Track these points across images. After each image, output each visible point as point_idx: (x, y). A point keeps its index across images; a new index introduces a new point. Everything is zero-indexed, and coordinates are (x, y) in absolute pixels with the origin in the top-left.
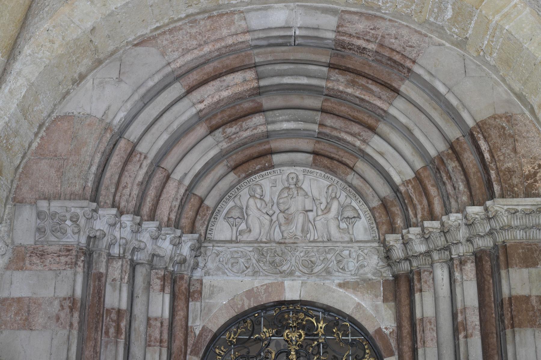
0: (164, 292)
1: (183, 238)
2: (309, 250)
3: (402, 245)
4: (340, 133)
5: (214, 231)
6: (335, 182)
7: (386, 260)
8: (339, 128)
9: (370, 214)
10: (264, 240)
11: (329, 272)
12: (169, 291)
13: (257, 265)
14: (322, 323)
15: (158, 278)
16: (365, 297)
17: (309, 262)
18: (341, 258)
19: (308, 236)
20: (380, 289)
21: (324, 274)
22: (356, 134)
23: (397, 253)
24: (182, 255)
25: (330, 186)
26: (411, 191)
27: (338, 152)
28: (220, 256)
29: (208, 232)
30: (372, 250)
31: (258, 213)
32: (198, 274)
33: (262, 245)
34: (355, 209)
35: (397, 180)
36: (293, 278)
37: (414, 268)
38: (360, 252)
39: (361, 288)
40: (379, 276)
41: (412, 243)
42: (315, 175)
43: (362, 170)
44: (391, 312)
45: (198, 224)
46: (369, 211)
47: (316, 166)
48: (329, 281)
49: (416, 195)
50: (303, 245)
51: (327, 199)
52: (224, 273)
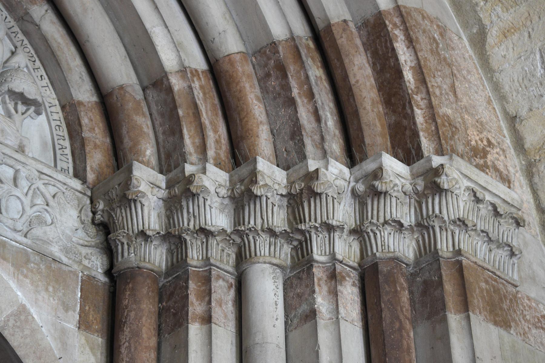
20: (75, 294)
23: (146, 218)
39: (32, 271)
41: (205, 200)
49: (206, 107)
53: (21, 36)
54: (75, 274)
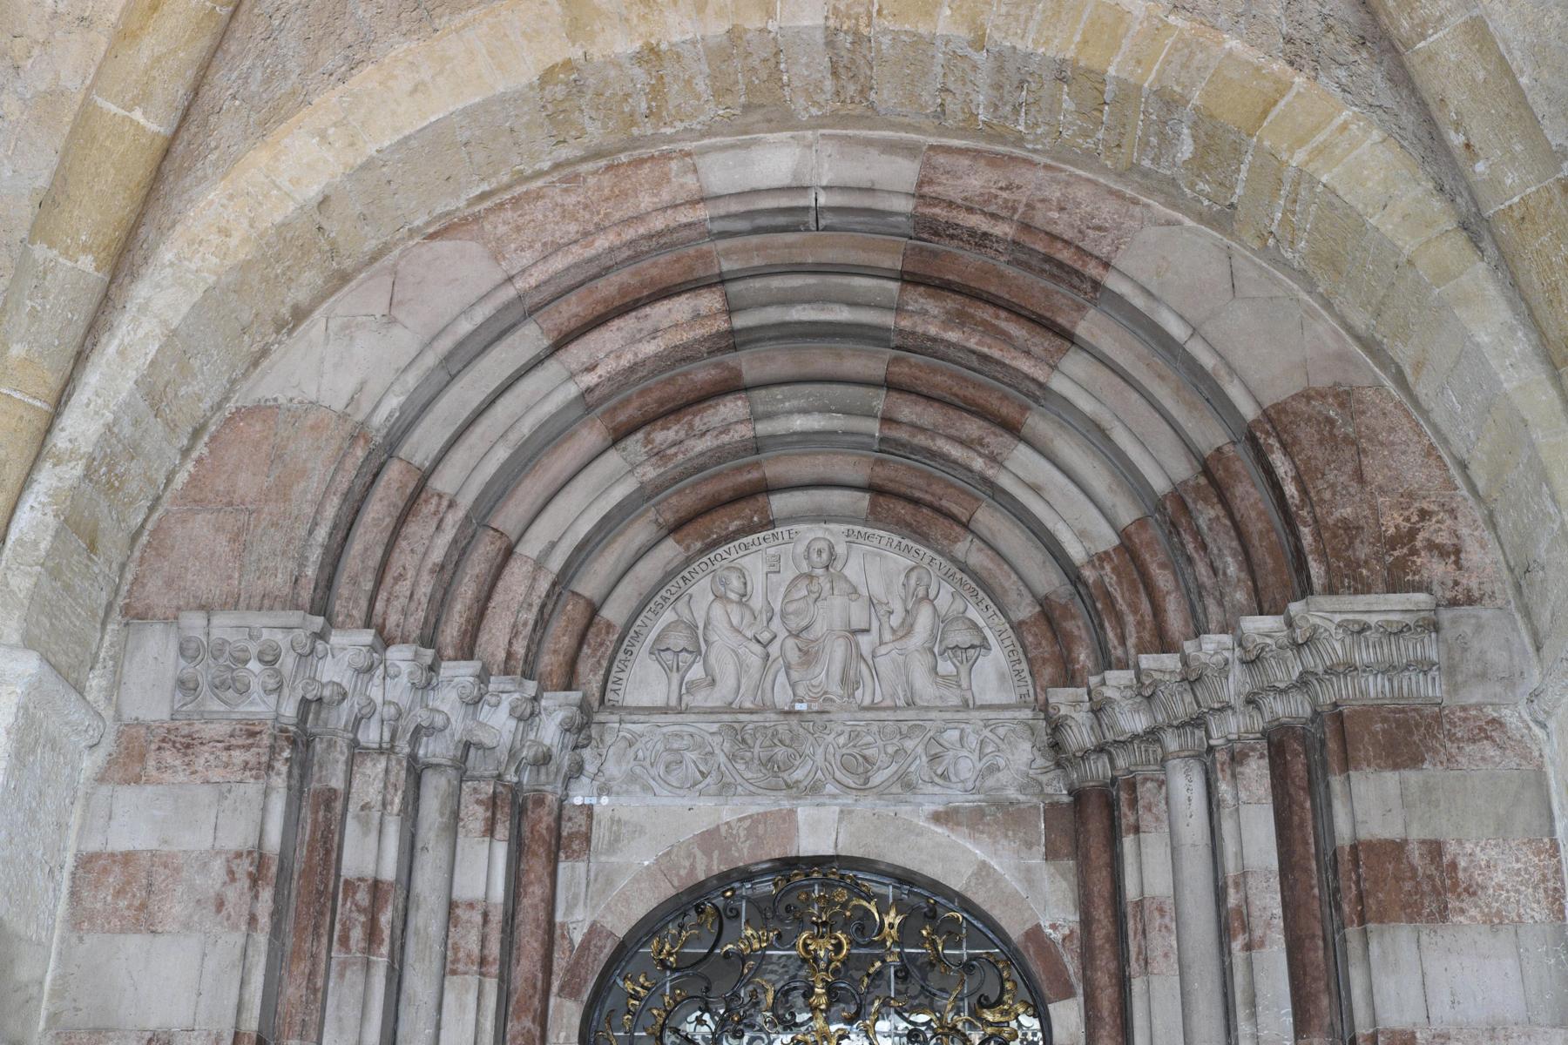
0: (492, 836)
1: (543, 703)
2: (859, 729)
3: (1090, 714)
4: (933, 440)
5: (624, 682)
6: (927, 560)
8: (931, 427)
9: (1013, 637)
10: (748, 705)
11: (909, 786)
12: (507, 833)
13: (730, 767)
14: (893, 914)
15: (478, 802)
16: (1000, 847)
17: (860, 759)
18: (939, 749)
19: (858, 693)
20: (1037, 826)
21: (896, 789)
22: (972, 441)
24: (540, 744)
25: (912, 569)
26: (1110, 579)
27: (929, 485)
28: (638, 745)
29: (610, 686)
30: (1018, 728)
31: (734, 640)
33: (742, 717)
34: (975, 626)
35: (1076, 552)
36: (820, 800)
37: (1121, 773)
38: (986, 732)
40: (1034, 795)
42: (876, 542)
43: (990, 530)
44: (1064, 885)
45: (584, 668)
46: (1010, 630)
47: (877, 520)
48: (908, 808)
49: (1122, 589)
50: (846, 716)
52: (647, 788)
54: (1036, 807)
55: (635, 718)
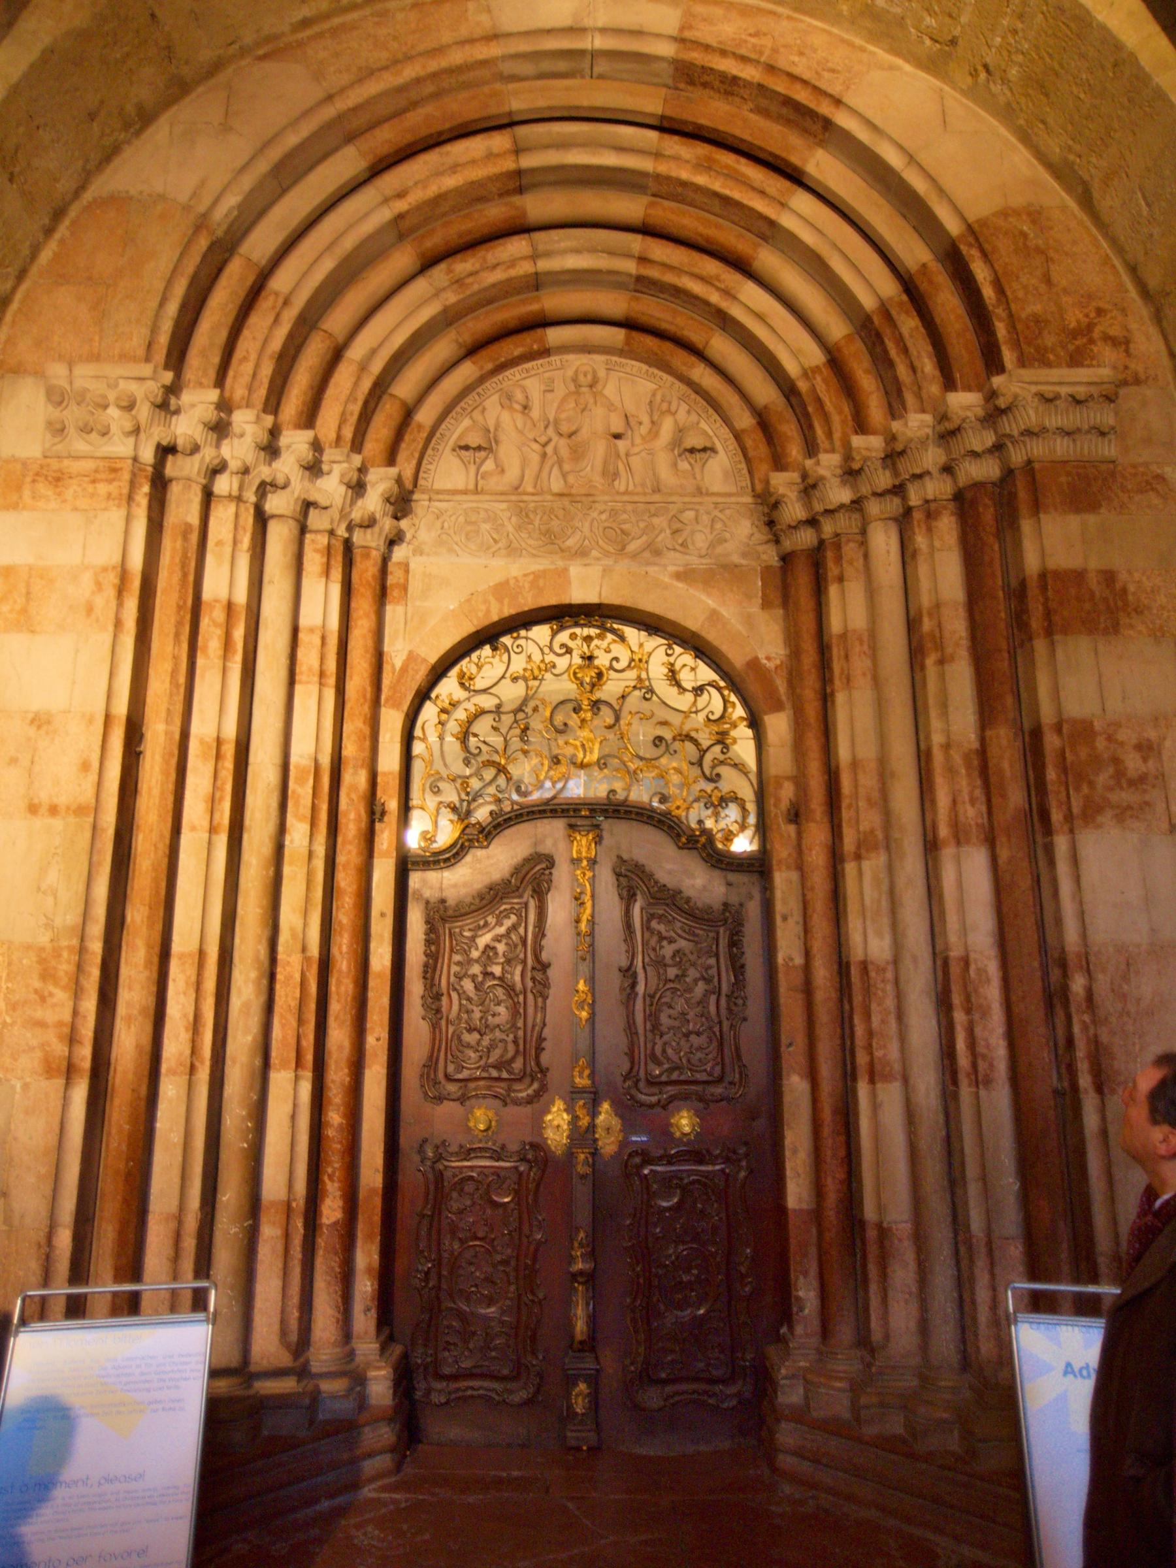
6: (668, 385)
7: (767, 528)
10: (530, 489)
18: (679, 525)
19: (616, 483)
21: (647, 554)
29: (421, 475)
32: (399, 553)
33: (525, 498)
34: (705, 433)
36: (586, 561)
38: (716, 513)
45: (402, 456)
48: (656, 568)
50: (606, 498)
51: (651, 416)
52: (451, 550)
53: (693, 396)
55: (441, 497)
